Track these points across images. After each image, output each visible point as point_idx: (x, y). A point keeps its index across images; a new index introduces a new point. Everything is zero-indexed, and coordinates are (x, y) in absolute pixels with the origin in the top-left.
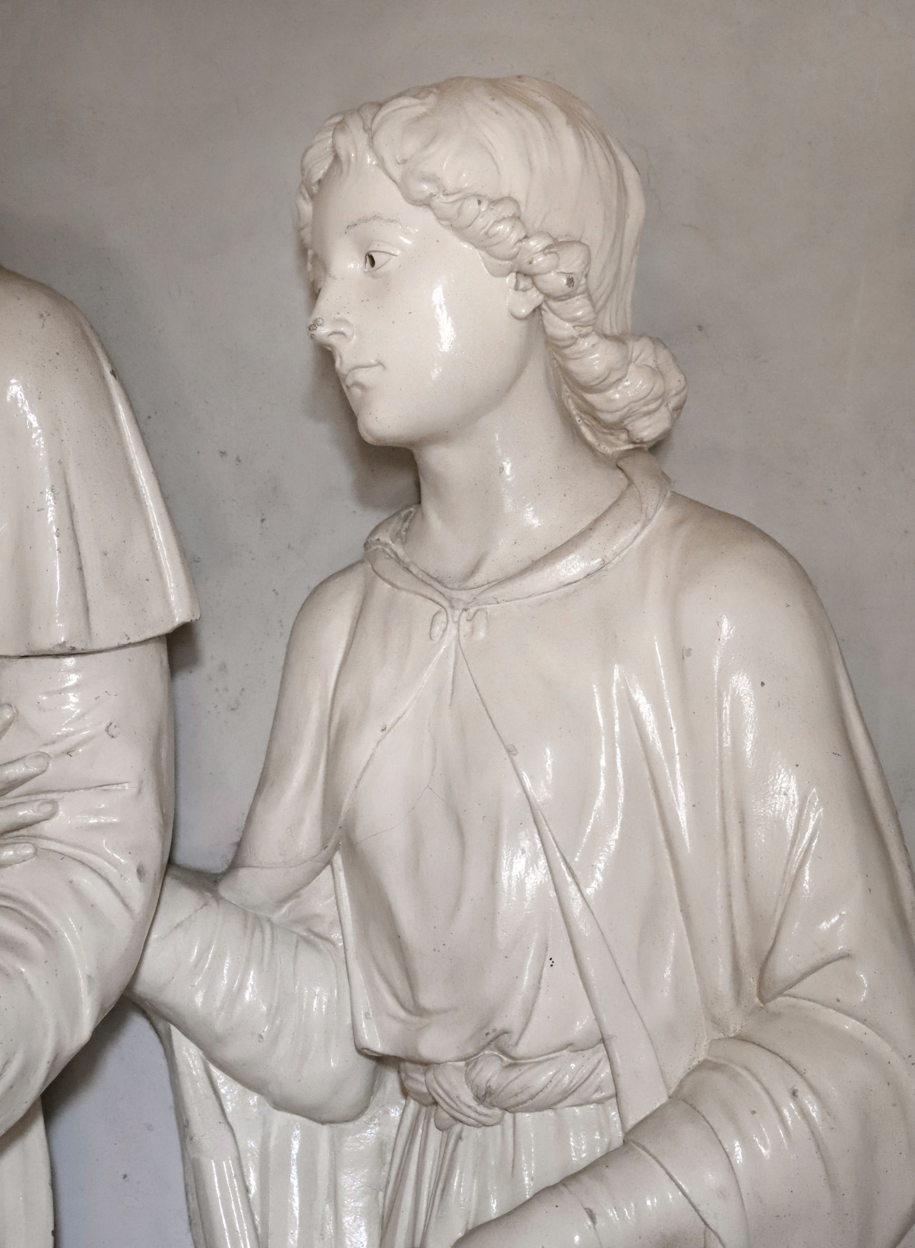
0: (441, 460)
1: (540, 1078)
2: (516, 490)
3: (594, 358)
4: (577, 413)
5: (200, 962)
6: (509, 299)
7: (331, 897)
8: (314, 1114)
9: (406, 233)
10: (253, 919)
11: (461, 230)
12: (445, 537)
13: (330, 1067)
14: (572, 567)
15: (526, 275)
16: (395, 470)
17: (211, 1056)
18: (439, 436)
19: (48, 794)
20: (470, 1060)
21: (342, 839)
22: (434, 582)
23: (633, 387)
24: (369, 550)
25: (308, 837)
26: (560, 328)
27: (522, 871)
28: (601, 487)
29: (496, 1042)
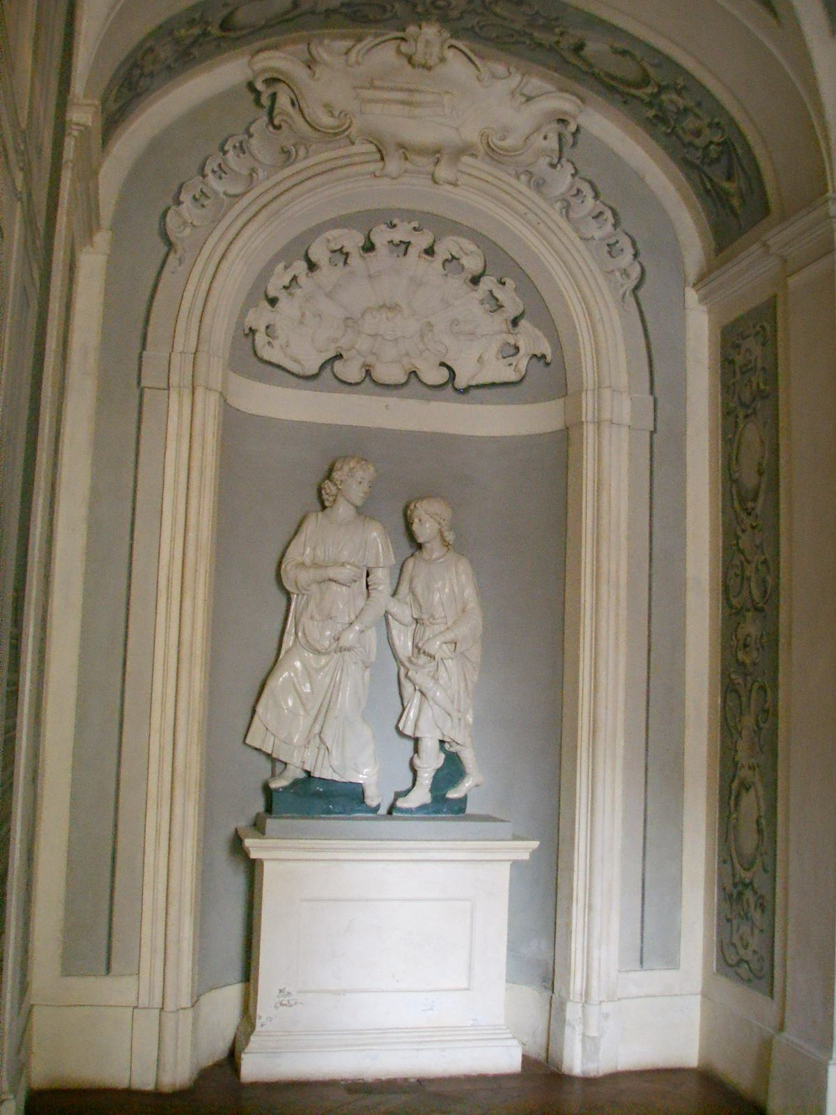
0: (428, 545)
1: (438, 621)
2: (434, 549)
3: (446, 534)
4: (443, 539)
5: (395, 607)
6: (437, 527)
7: (409, 599)
8: (406, 626)
9: (425, 517)
10: (399, 600)
11: (431, 517)
12: (425, 554)
13: (408, 619)
14: (441, 560)
15: (440, 524)
16: (420, 547)
17: (393, 617)
18: (425, 542)
19: (380, 584)
20: (428, 620)
21: (412, 591)
22: (425, 560)
23: (450, 537)
24: (412, 555)
25: (407, 591)
26: (443, 530)
27: (437, 596)
28: (446, 549)
29: (432, 616)
